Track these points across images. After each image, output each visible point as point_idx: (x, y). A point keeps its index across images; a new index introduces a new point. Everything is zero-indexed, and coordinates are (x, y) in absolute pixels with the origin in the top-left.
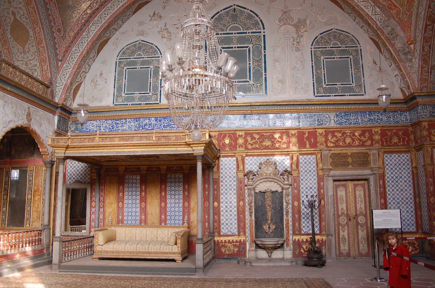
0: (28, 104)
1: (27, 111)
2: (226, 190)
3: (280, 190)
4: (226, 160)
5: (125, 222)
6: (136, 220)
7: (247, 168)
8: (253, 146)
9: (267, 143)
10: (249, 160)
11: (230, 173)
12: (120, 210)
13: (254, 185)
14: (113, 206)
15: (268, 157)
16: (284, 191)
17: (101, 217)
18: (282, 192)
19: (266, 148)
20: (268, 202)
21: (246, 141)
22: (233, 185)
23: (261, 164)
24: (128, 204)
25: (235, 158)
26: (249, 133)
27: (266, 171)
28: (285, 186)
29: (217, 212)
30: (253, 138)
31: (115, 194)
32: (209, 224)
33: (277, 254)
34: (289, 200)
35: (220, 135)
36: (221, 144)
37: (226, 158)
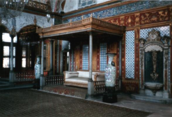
0: (35, 15)
1: (34, 18)
2: (129, 51)
3: (161, 51)
4: (129, 33)
5: (83, 69)
6: (87, 68)
7: (141, 37)
8: (145, 22)
9: (154, 19)
10: (142, 31)
11: (131, 40)
12: (81, 62)
13: (144, 48)
14: (78, 61)
15: (154, 28)
16: (164, 51)
17: (74, 66)
18: (163, 52)
19: (153, 22)
20: (154, 59)
21: (141, 19)
22: (132, 48)
23: (149, 33)
24: (84, 59)
25: (134, 31)
26: (143, 14)
27: (152, 38)
28: (165, 48)
29: (123, 64)
30: (145, 16)
31: (79, 55)
32: (119, 71)
33: (158, 94)
34: (169, 57)
35: (125, 17)
36: (126, 23)
37: (129, 32)
